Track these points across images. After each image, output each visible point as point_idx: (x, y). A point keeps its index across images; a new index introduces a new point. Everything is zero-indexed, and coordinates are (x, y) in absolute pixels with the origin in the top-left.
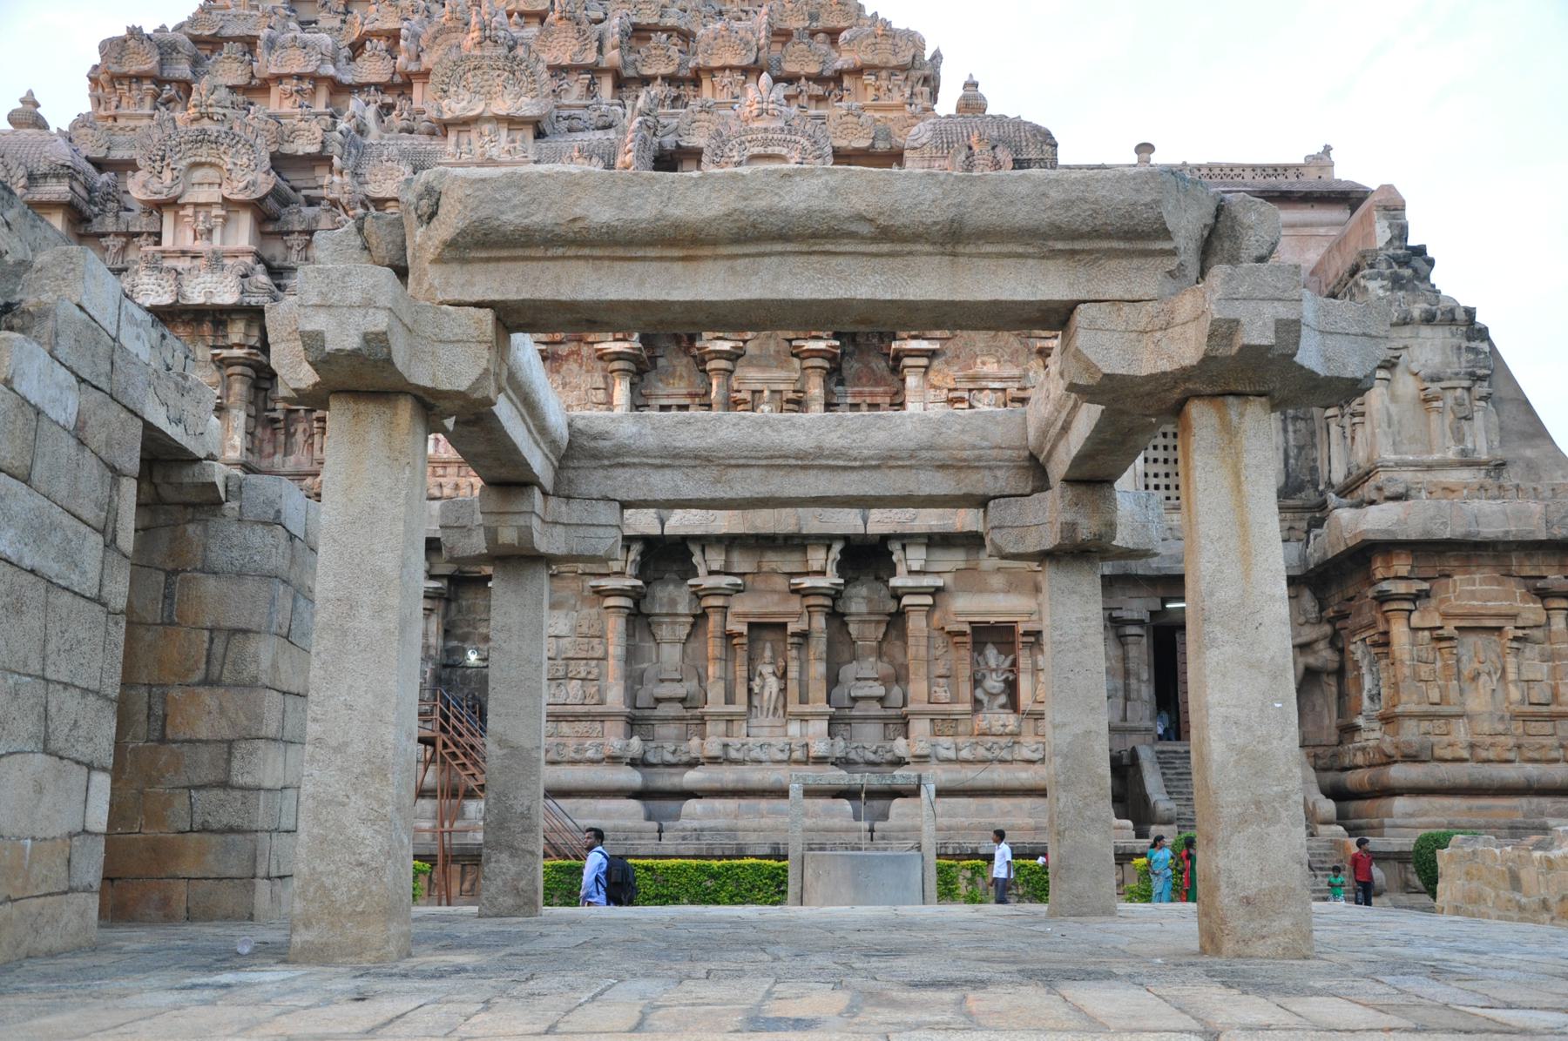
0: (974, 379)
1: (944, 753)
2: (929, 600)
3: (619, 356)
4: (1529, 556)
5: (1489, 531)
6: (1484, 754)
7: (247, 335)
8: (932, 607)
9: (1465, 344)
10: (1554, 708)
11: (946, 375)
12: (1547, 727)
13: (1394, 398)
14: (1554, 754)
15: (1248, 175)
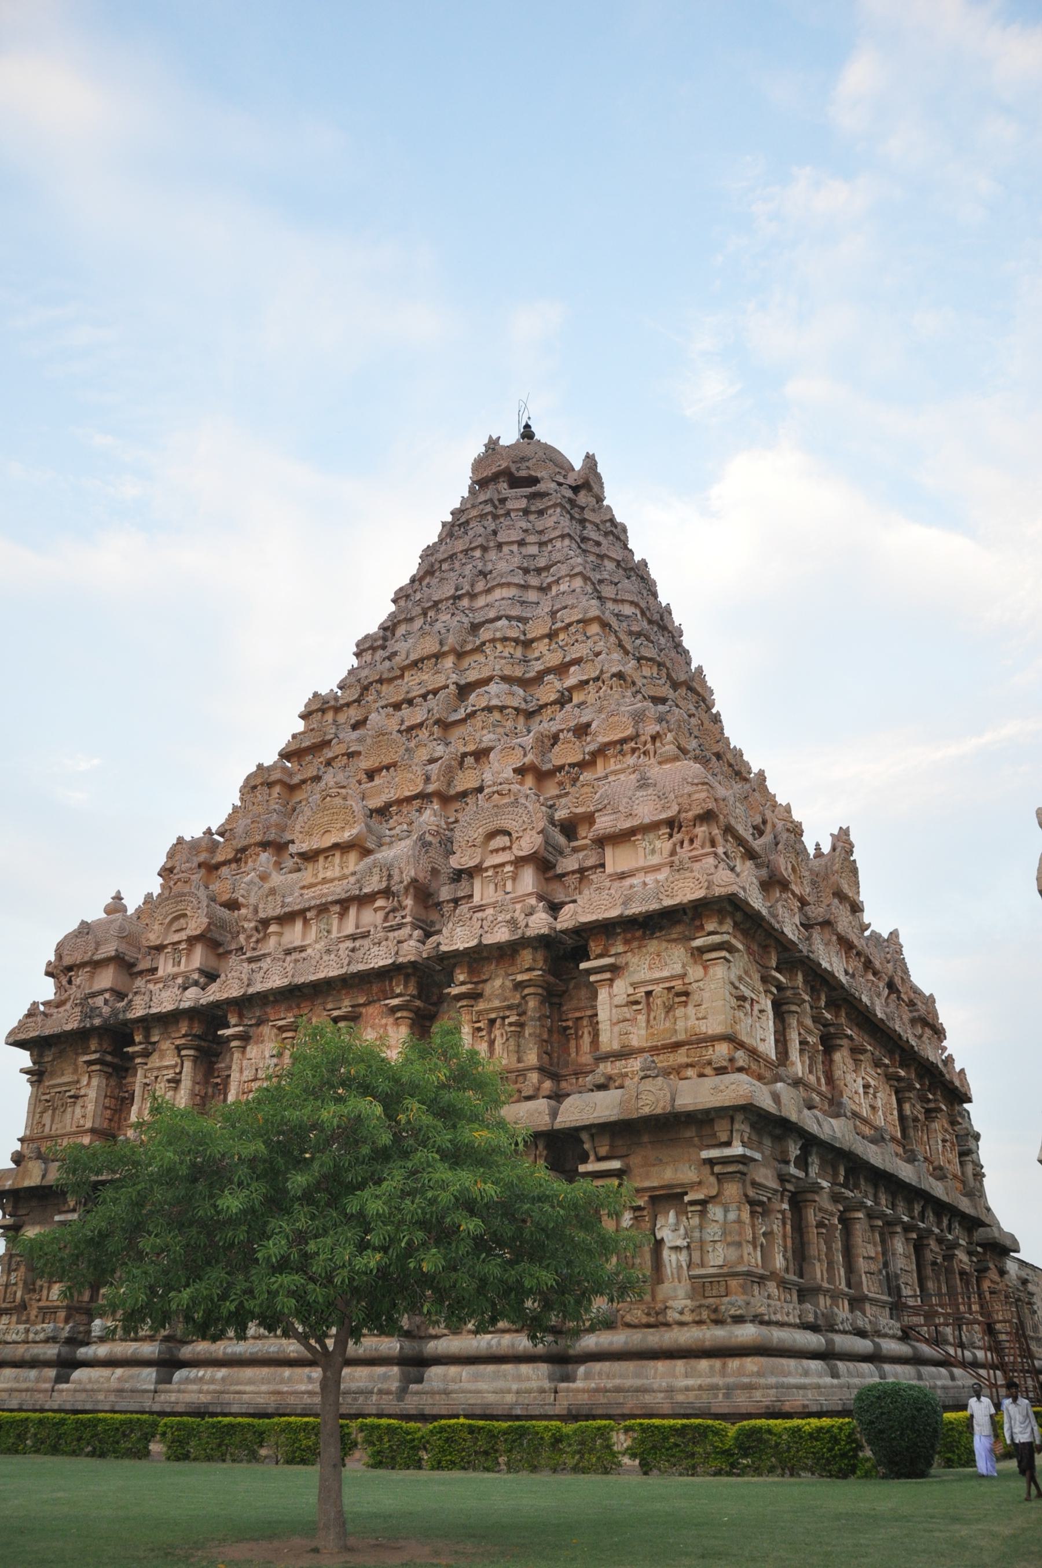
7: (191, 1028)
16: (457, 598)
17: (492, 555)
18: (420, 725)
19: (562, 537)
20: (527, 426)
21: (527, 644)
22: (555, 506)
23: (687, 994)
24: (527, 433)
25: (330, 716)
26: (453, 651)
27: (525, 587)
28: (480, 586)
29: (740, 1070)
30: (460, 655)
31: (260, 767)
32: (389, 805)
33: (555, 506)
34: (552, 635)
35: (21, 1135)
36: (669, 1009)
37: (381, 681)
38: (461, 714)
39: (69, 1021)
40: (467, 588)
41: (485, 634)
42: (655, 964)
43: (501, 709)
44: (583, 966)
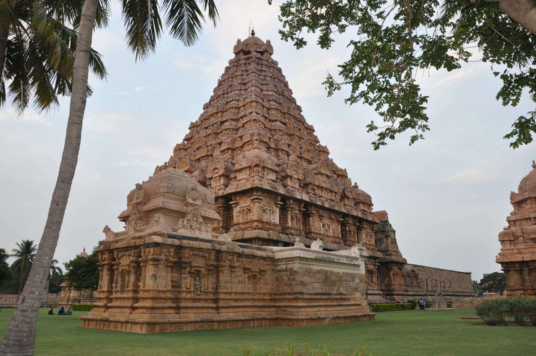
16: (223, 94)
18: (210, 134)
19: (252, 72)
20: (253, 31)
21: (239, 108)
22: (253, 61)
23: (250, 210)
24: (253, 34)
25: (195, 129)
26: (221, 111)
27: (241, 90)
28: (229, 91)
29: (259, 229)
30: (223, 112)
31: (177, 144)
32: (200, 158)
33: (253, 61)
34: (244, 106)
36: (247, 214)
37: (205, 119)
38: (219, 131)
40: (226, 91)
41: (228, 107)
42: (244, 203)
43: (229, 129)
44: (230, 203)
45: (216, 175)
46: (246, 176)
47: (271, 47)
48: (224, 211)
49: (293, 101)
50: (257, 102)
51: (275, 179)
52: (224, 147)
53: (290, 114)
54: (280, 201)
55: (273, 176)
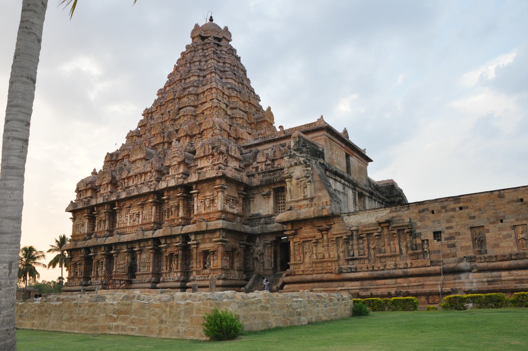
0: (205, 197)
1: (197, 279)
2: (195, 246)
3: (151, 202)
4: (318, 221)
5: (302, 217)
6: (306, 273)
7: (107, 207)
8: (197, 248)
9: (305, 169)
10: (324, 260)
11: (201, 197)
12: (321, 265)
13: (292, 185)
14: (321, 272)
15: (304, 128)
17: (192, 65)
20: (211, 17)
24: (211, 20)
26: (178, 98)
31: (131, 131)
32: (155, 145)
35: (71, 235)
39: (80, 206)
45: (175, 163)
46: (208, 164)
47: (230, 34)
48: (183, 200)
49: (252, 91)
50: (217, 89)
51: (238, 168)
52: (181, 134)
53: (249, 103)
54: (244, 191)
55: (236, 164)
